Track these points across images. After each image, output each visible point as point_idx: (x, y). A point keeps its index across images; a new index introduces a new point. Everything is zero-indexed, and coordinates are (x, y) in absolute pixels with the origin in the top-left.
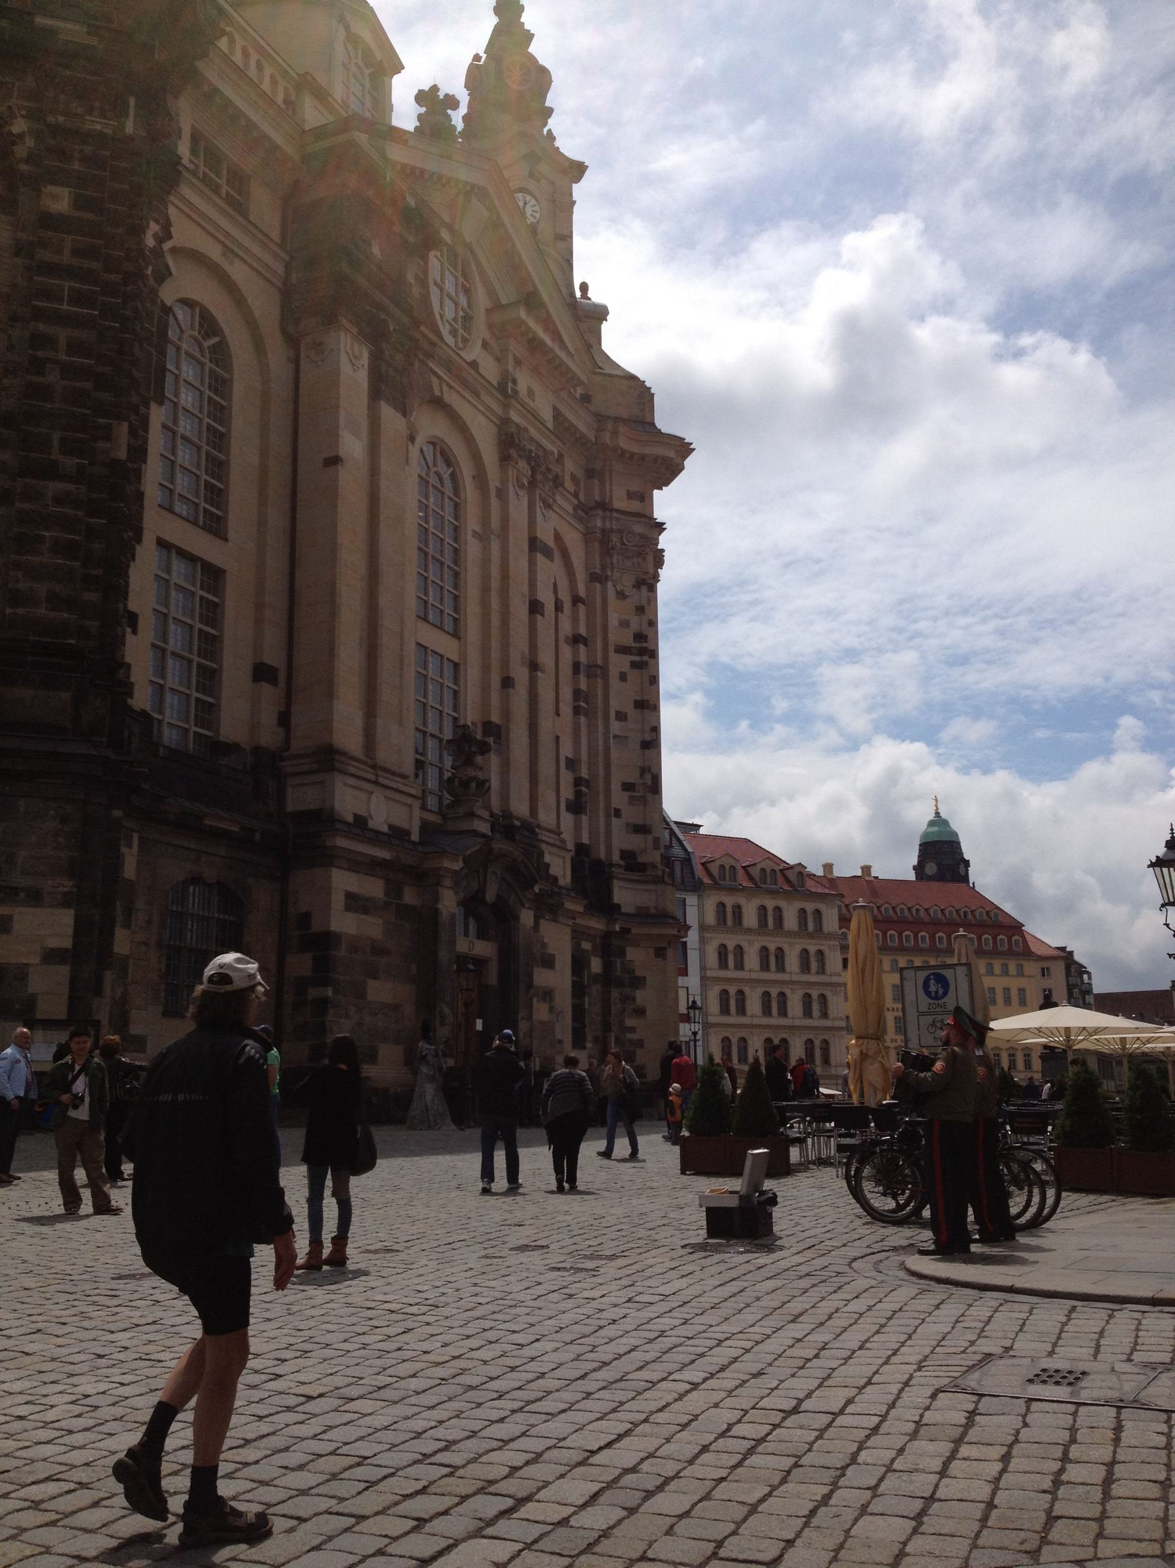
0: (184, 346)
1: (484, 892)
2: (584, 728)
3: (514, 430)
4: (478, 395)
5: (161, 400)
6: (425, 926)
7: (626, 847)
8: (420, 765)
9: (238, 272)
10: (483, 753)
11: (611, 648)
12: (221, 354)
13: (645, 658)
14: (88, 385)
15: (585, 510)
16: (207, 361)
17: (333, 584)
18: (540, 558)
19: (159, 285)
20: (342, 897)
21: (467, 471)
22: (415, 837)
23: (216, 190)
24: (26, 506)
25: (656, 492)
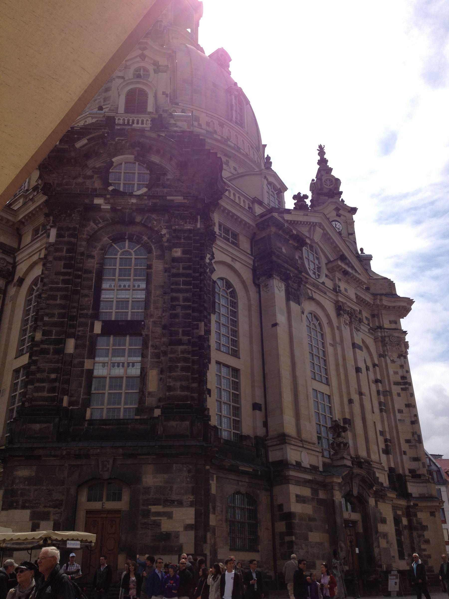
0: (221, 293)
1: (352, 491)
3: (341, 304)
5: (214, 312)
6: (329, 507)
8: (319, 438)
9: (237, 266)
11: (392, 384)
12: (233, 294)
13: (407, 386)
14: (190, 311)
15: (373, 330)
17: (279, 370)
18: (357, 350)
20: (294, 497)
21: (325, 321)
22: (321, 469)
23: (228, 240)
24: (172, 356)
25: (401, 320)
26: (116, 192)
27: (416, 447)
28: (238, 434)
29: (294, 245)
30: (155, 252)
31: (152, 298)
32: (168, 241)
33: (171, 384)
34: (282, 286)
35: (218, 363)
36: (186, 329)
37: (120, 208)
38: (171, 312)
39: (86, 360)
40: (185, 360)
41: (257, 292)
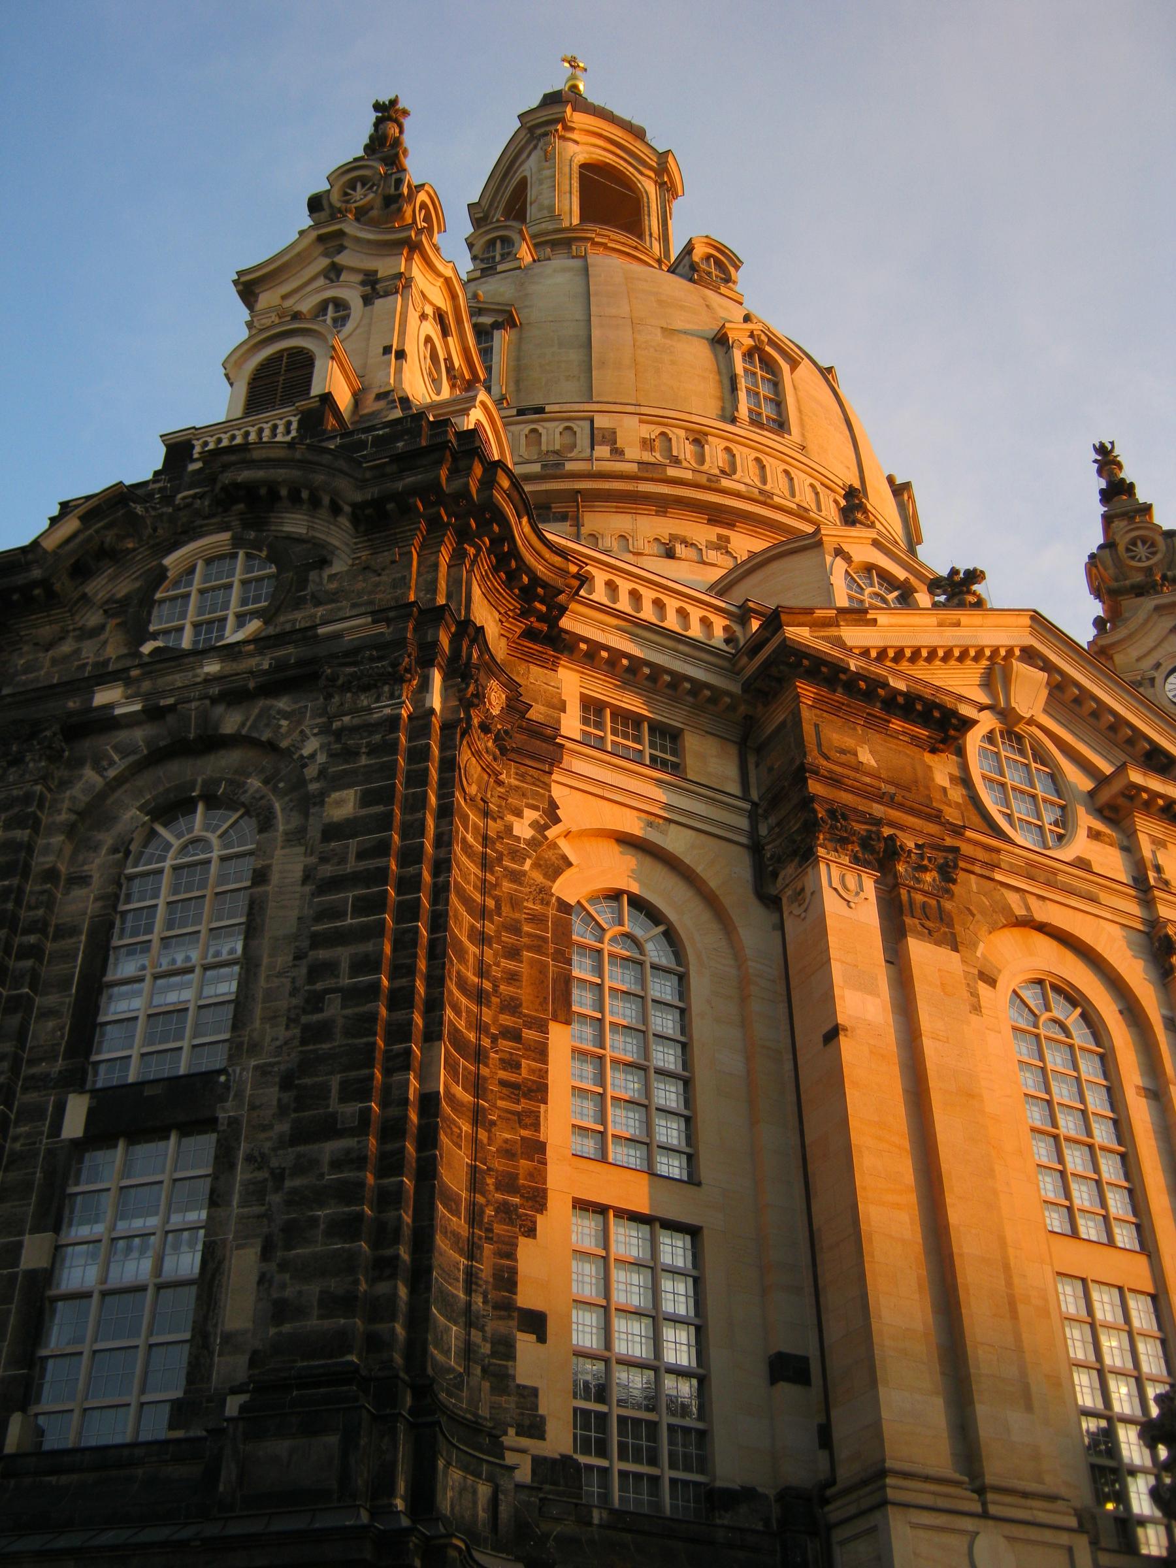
0: (606, 947)
4: (1093, 899)
5: (566, 1016)
24: (298, 1182)
26: (170, 658)
28: (697, 1484)
29: (914, 738)
30: (282, 825)
31: (262, 982)
32: (322, 773)
33: (288, 1293)
35: (582, 1206)
36: (353, 1074)
37: (171, 701)
38: (305, 1019)
39: (27, 1236)
41: (774, 928)
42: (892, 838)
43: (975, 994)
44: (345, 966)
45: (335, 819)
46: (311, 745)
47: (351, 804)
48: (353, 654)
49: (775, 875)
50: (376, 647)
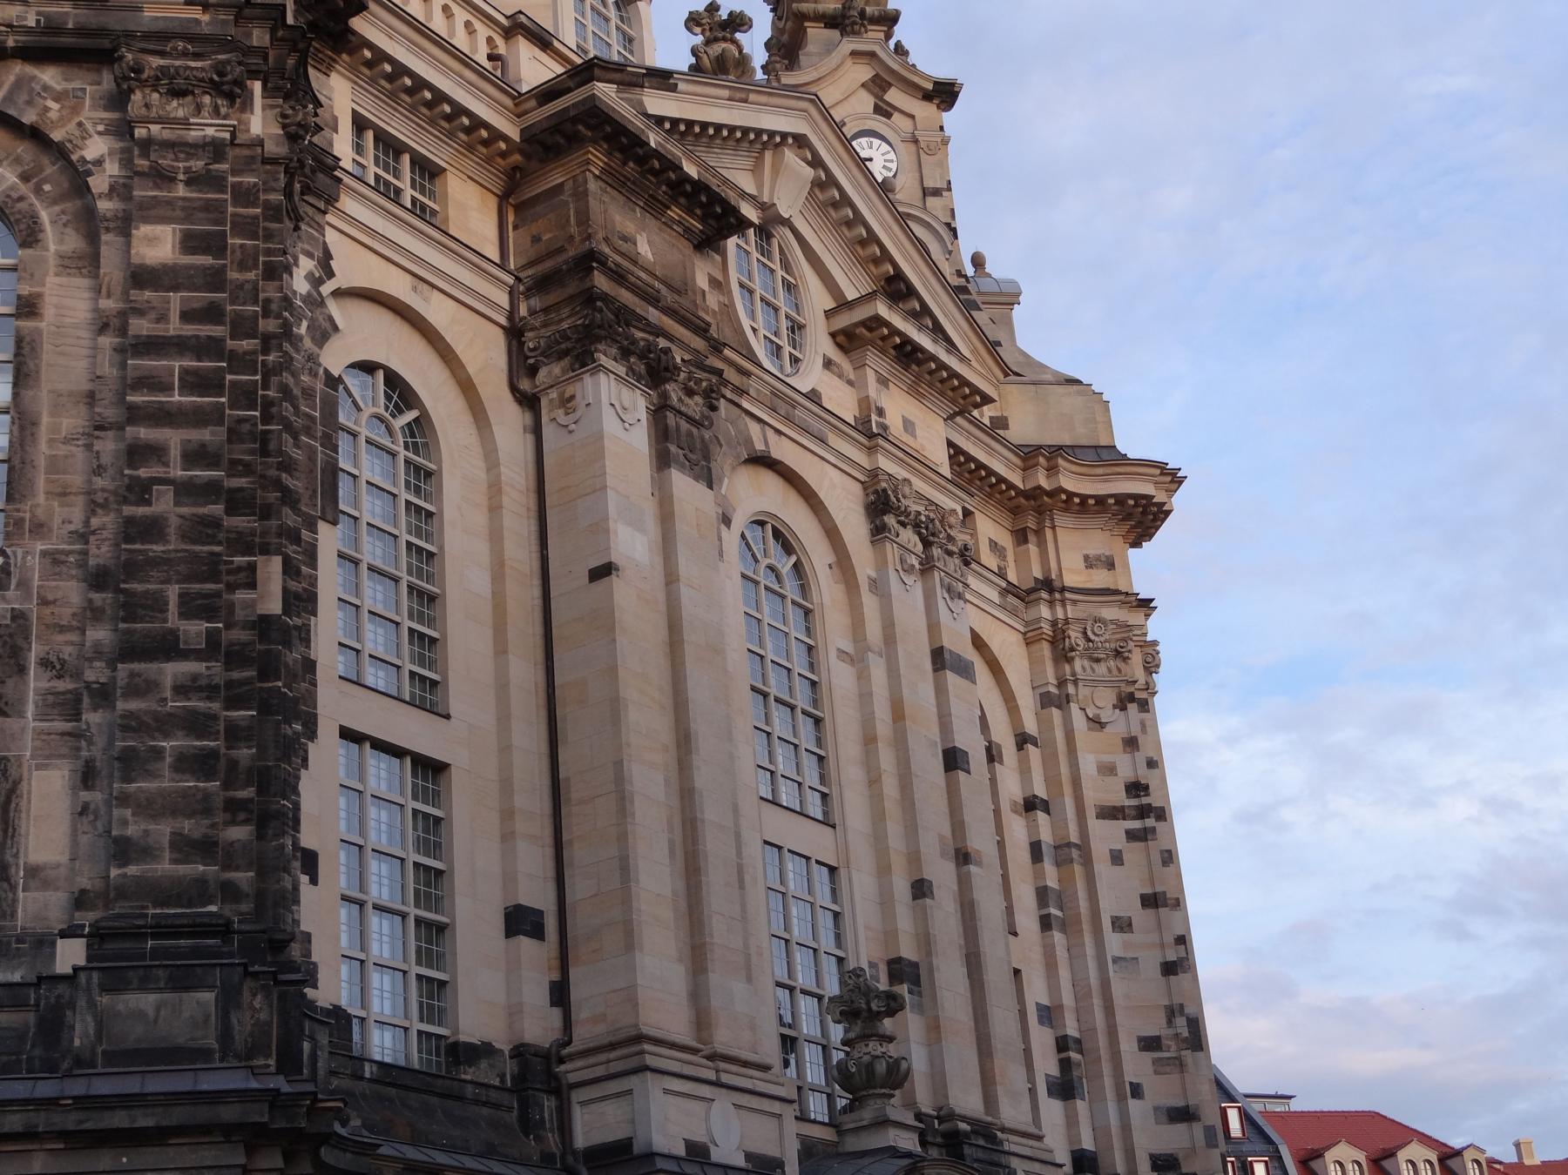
0: (364, 432)
2: (1061, 953)
7: (1161, 1148)
8: (789, 1043)
9: (437, 311)
10: (891, 1013)
11: (1091, 814)
13: (1150, 822)
14: (217, 509)
15: (1022, 595)
16: (401, 449)
17: (619, 764)
18: (951, 677)
19: (321, 348)
21: (819, 555)
23: (395, 195)
24: (134, 705)
27: (1180, 1065)
28: (439, 1037)
29: (687, 230)
32: (119, 190)
33: (132, 831)
34: (638, 403)
35: (348, 734)
36: (196, 587)
38: (128, 510)
40: (196, 724)
42: (667, 351)
43: (720, 539)
44: (175, 453)
45: (148, 262)
46: (96, 148)
47: (169, 246)
48: (160, 38)
49: (533, 372)
50: (190, 38)
